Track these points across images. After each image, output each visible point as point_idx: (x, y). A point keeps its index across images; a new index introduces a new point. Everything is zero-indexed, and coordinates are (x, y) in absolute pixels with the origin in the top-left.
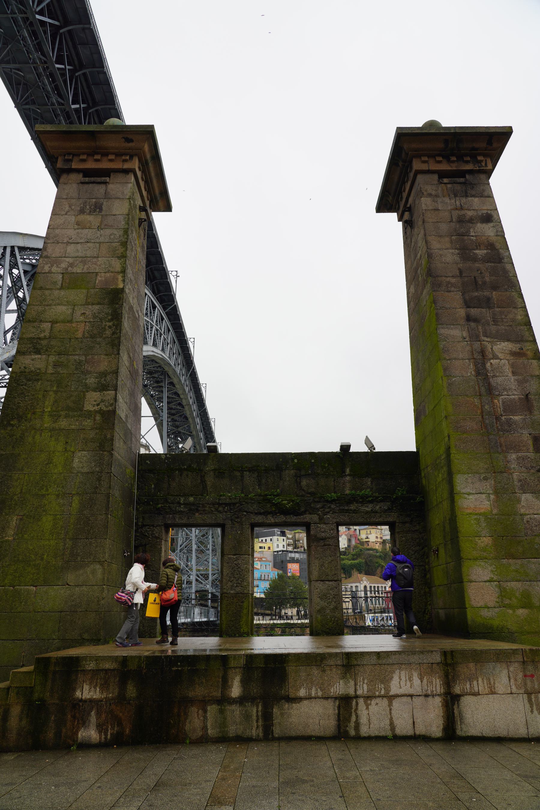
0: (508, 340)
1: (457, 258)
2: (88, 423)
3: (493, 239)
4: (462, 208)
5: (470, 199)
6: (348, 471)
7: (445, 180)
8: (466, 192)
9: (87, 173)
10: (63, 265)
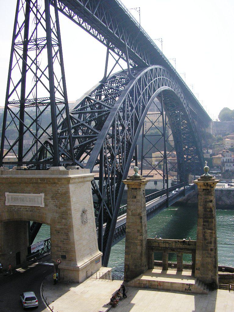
0: (210, 230)
2: (139, 241)
9: (132, 189)
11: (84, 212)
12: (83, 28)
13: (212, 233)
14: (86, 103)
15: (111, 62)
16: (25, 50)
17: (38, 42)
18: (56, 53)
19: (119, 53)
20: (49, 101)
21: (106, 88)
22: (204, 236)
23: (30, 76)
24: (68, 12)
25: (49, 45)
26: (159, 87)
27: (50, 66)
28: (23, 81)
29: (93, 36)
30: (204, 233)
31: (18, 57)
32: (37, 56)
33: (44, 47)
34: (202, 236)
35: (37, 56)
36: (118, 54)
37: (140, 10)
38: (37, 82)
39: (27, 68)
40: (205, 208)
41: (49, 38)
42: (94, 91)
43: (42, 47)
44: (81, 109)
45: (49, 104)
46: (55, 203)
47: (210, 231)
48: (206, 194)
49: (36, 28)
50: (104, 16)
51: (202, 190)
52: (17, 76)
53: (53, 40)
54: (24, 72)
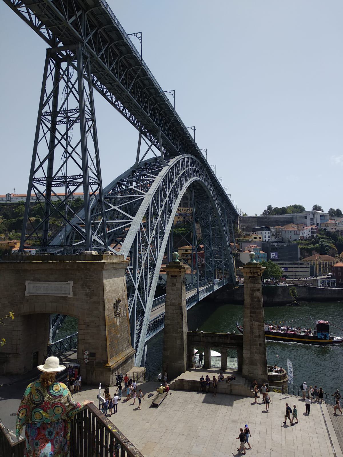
1: (250, 301)
2: (179, 335)
3: (259, 296)
4: (253, 287)
5: (255, 284)
6: (229, 338)
7: (250, 279)
8: (255, 282)
9: (172, 276)
10: (171, 300)
11: (118, 302)
12: (115, 106)
13: (260, 325)
14: (117, 189)
15: (144, 147)
16: (54, 123)
17: (69, 114)
18: (90, 128)
19: (151, 138)
20: (81, 180)
21: (138, 174)
22: (251, 328)
23: (59, 151)
24: (100, 86)
25: (81, 120)
26: (190, 177)
27: (83, 141)
28: (50, 157)
29: (126, 117)
30: (251, 325)
31: (46, 129)
32: (68, 130)
33: (75, 122)
34: (249, 329)
35: (68, 130)
36: (150, 140)
37: (174, 94)
38: (67, 158)
39: (56, 142)
40: (252, 297)
41: (81, 110)
42: (125, 177)
43: (73, 121)
44: (111, 195)
45: (80, 184)
46: (85, 292)
47: (258, 323)
48: (252, 283)
49: (67, 99)
50: (139, 96)
51: (248, 277)
52: (43, 151)
53: (87, 113)
54: (52, 147)
